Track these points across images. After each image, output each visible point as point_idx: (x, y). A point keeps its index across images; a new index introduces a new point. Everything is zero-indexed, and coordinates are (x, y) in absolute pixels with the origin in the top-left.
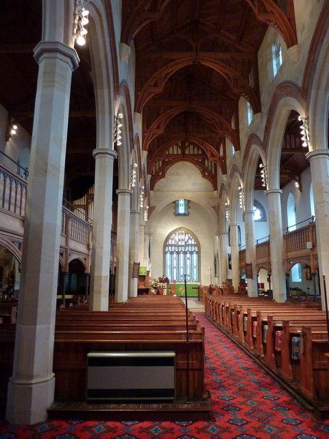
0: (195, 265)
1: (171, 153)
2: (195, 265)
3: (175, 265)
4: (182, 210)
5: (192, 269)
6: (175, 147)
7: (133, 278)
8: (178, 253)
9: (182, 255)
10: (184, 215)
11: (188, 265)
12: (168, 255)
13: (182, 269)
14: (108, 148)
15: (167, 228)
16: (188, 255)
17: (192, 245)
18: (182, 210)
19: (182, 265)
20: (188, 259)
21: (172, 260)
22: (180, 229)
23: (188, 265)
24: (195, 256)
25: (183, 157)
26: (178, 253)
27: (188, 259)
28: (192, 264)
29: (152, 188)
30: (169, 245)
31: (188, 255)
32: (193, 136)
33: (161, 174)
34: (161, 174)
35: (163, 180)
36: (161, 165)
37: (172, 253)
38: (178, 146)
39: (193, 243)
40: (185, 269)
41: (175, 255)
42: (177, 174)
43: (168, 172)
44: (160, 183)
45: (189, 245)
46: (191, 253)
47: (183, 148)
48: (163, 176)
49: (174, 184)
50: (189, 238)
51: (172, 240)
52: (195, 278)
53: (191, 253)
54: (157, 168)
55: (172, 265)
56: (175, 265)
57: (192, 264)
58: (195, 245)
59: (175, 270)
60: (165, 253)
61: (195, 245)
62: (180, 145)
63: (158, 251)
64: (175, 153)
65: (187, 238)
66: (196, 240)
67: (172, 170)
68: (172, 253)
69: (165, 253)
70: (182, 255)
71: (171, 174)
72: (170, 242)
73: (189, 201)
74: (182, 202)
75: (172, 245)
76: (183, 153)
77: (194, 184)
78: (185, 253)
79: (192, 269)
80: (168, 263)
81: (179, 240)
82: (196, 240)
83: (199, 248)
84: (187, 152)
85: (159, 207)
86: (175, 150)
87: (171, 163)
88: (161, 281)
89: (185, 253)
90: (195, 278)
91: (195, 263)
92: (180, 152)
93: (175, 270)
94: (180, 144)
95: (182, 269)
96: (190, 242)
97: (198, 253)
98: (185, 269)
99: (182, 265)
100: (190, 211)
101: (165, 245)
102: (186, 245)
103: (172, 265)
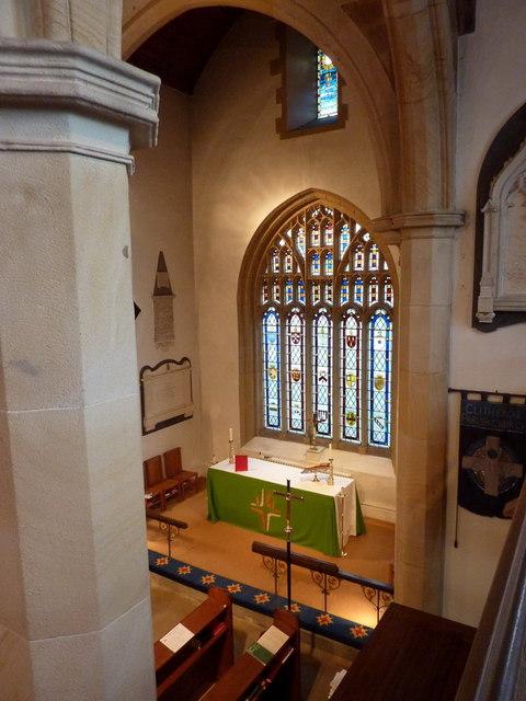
0: (380, 372)
2: (380, 372)
3: (296, 366)
4: (328, 108)
5: (365, 394)
8: (309, 314)
9: (323, 321)
11: (351, 370)
13: (323, 384)
16: (351, 327)
17: (367, 278)
19: (323, 369)
20: (352, 341)
21: (283, 347)
23: (351, 370)
26: (309, 314)
27: (352, 341)
28: (365, 368)
30: (272, 280)
31: (351, 327)
37: (284, 314)
45: (353, 279)
46: (366, 316)
50: (356, 240)
51: (284, 252)
53: (366, 316)
55: (284, 361)
56: (296, 366)
57: (365, 368)
59: (296, 388)
60: (251, 317)
65: (346, 240)
68: (284, 314)
69: (251, 317)
70: (323, 321)
78: (338, 315)
79: (365, 394)
81: (311, 255)
89: (338, 315)
93: (296, 388)
95: (323, 384)
96: (359, 264)
99: (323, 369)
102: (339, 280)
103: (284, 361)
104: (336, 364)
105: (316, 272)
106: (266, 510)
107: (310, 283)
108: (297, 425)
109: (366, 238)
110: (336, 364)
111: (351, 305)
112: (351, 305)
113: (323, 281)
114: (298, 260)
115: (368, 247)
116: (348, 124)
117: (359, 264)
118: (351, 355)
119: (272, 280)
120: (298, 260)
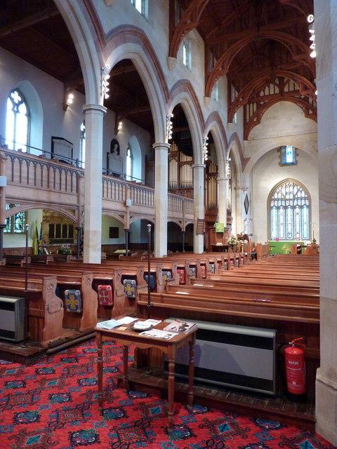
1: (267, 93)
4: (289, 159)
6: (272, 86)
7: (197, 234)
8: (285, 208)
10: (292, 164)
12: (274, 211)
13: (289, 225)
14: (94, 103)
15: (270, 180)
16: (297, 210)
17: (301, 199)
18: (289, 159)
22: (287, 180)
24: (305, 211)
25: (282, 96)
26: (285, 208)
28: (301, 221)
29: (245, 138)
30: (275, 200)
31: (297, 210)
32: (281, 69)
33: (255, 120)
34: (255, 120)
35: (258, 126)
36: (255, 110)
37: (278, 208)
38: (275, 84)
39: (303, 195)
40: (294, 225)
41: (282, 210)
42: (274, 117)
43: (264, 118)
44: (255, 131)
46: (301, 207)
47: (281, 86)
48: (258, 122)
49: (270, 130)
50: (299, 190)
52: (305, 236)
53: (301, 207)
54: (251, 115)
55: (278, 221)
57: (301, 221)
58: (305, 198)
60: (269, 208)
61: (305, 198)
62: (278, 83)
63: (260, 208)
64: (272, 93)
65: (296, 190)
66: (307, 192)
67: (268, 113)
68: (278, 208)
69: (269, 208)
71: (267, 119)
72: (276, 196)
73: (296, 149)
74: (289, 150)
75: (278, 200)
76: (282, 91)
77: (296, 126)
78: (293, 207)
80: (274, 219)
82: (307, 192)
83: (310, 202)
84: (286, 90)
85: (254, 160)
86: (272, 90)
87: (267, 106)
88: (240, 238)
89: (293, 207)
90: (305, 236)
91: (306, 219)
92: (277, 90)
94: (277, 81)
95: (289, 225)
97: (309, 207)
98: (294, 225)
99: (289, 221)
100: (298, 158)
101: (270, 198)
103: (278, 221)
104: (293, 220)
105: (287, 197)
106: (286, 249)
107: (286, 200)
108: (282, 236)
109: (301, 189)
110: (293, 220)
111: (297, 205)
112: (297, 205)
113: (290, 200)
114: (282, 194)
115: (301, 192)
116: (299, 162)
117: (299, 194)
118: (297, 218)
119: (275, 200)
120: (282, 194)
